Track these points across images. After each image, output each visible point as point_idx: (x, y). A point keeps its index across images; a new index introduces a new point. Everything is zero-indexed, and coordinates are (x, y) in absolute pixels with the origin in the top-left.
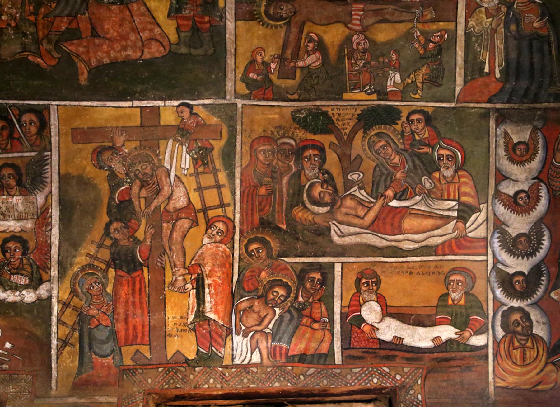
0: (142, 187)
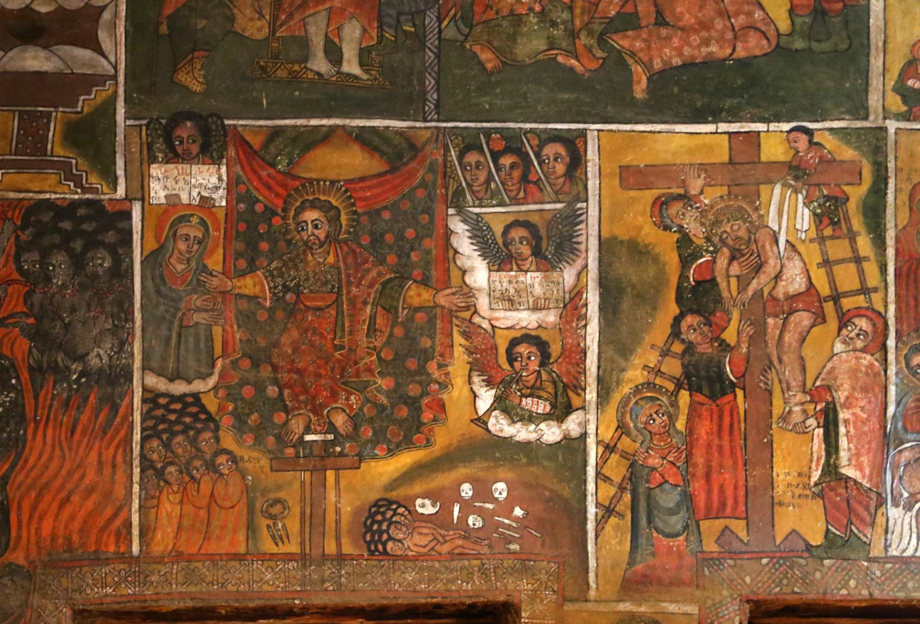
0: (733, 258)
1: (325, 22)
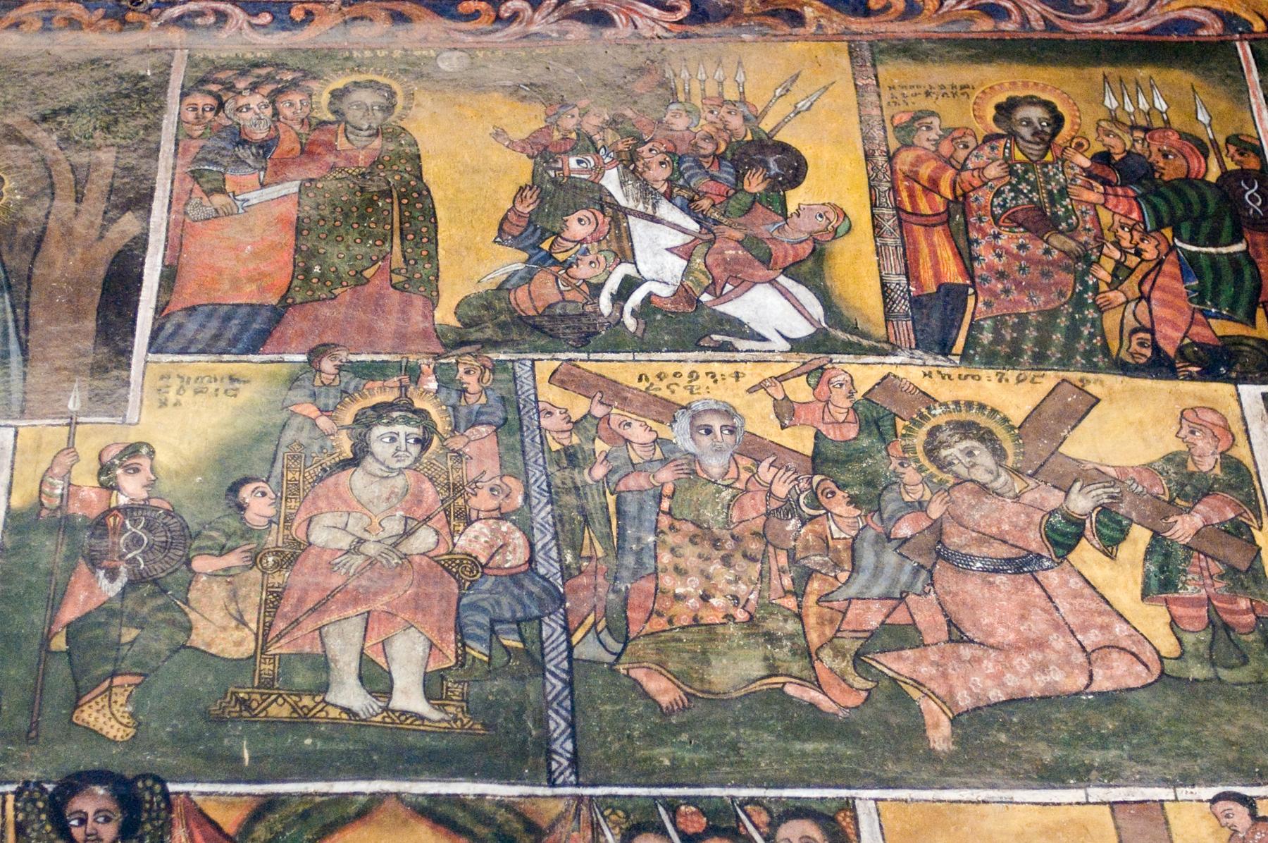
1: (358, 635)
